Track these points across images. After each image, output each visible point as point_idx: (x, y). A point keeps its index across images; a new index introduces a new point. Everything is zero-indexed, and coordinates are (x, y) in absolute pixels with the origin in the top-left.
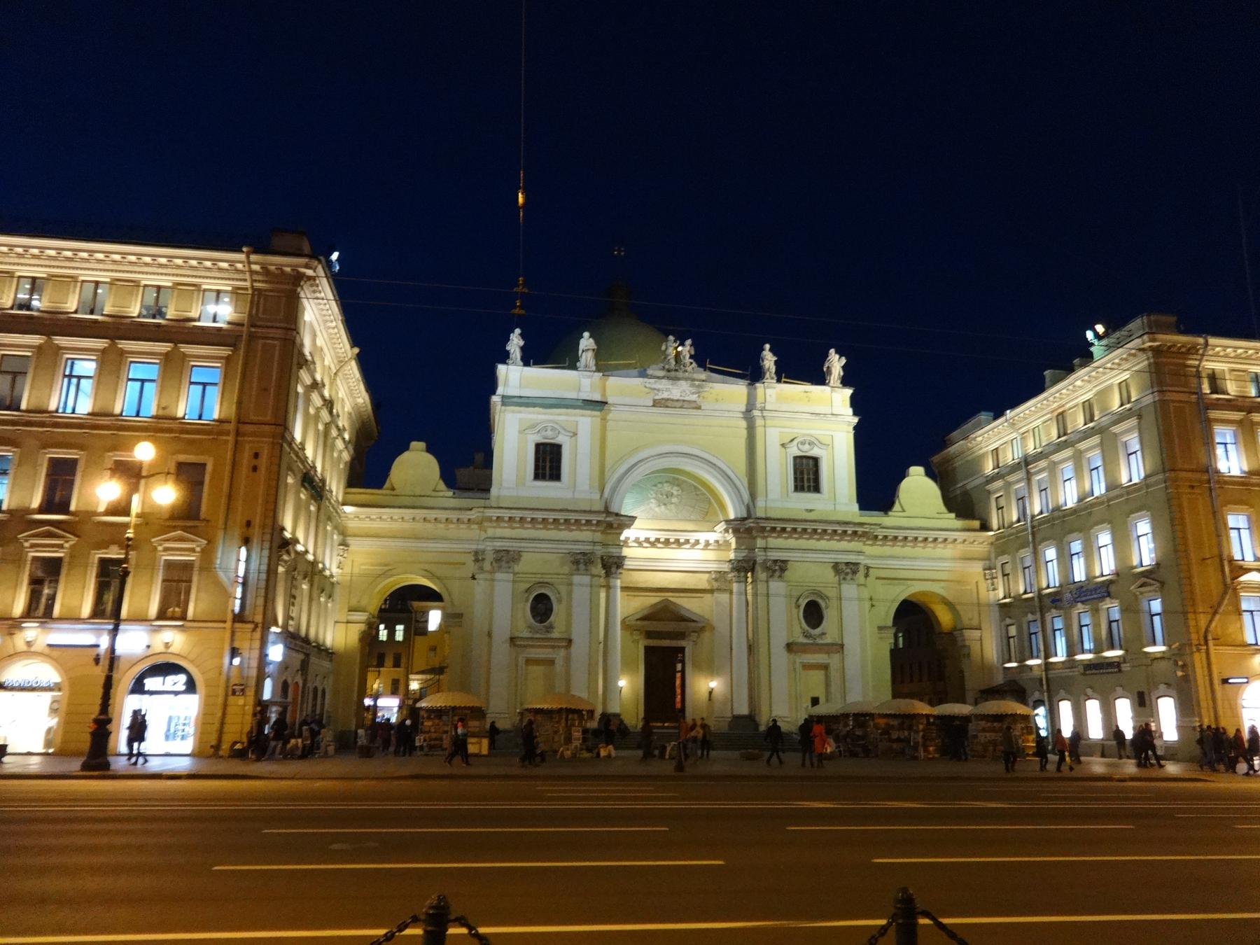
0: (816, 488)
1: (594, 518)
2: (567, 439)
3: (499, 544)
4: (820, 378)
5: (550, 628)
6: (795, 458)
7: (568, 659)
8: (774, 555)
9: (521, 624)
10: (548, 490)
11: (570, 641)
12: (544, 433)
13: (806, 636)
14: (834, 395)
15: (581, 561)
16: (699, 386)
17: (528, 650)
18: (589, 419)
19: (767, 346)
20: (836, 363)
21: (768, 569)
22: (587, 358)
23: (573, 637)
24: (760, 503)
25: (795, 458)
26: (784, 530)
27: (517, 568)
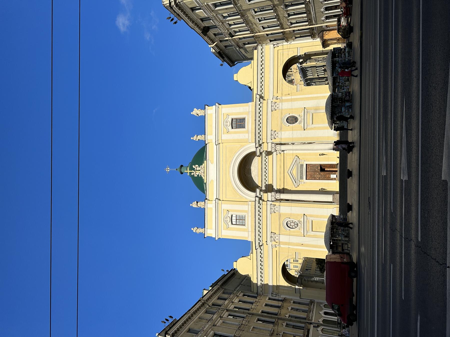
0: (243, 120)
1: (257, 205)
4: (203, 118)
7: (311, 216)
12: (229, 221)
14: (209, 113)
19: (192, 138)
20: (196, 112)
22: (201, 204)
27: (277, 233)
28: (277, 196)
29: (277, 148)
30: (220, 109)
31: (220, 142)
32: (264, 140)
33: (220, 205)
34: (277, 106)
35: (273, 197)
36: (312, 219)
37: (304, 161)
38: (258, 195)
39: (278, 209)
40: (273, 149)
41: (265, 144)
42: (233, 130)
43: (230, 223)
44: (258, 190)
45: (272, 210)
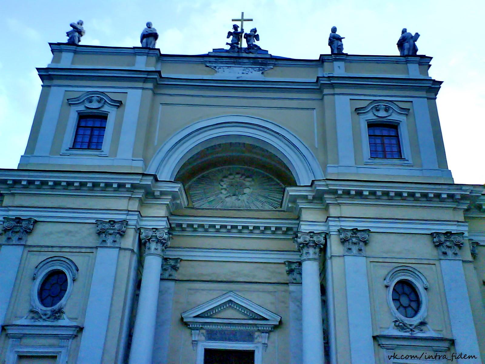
2: (115, 109)
3: (13, 214)
5: (57, 314)
6: (371, 125)
8: (349, 225)
9: (23, 308)
10: (87, 160)
11: (81, 329)
13: (399, 326)
15: (108, 231)
16: (262, 64)
17: (25, 341)
18: (140, 91)
21: (344, 241)
23: (86, 325)
24: (330, 170)
25: (371, 125)
26: (359, 194)
28: (153, 246)
29: (311, 250)
30: (423, 94)
31: (326, 91)
32: (334, 211)
33: (140, 85)
34: (450, 252)
35: (150, 233)
36: (62, 359)
37: (265, 345)
38: (166, 187)
39: (109, 245)
40: (308, 238)
41: (319, 216)
42: (364, 126)
43: (81, 108)
44: (177, 187)
45: (107, 226)
